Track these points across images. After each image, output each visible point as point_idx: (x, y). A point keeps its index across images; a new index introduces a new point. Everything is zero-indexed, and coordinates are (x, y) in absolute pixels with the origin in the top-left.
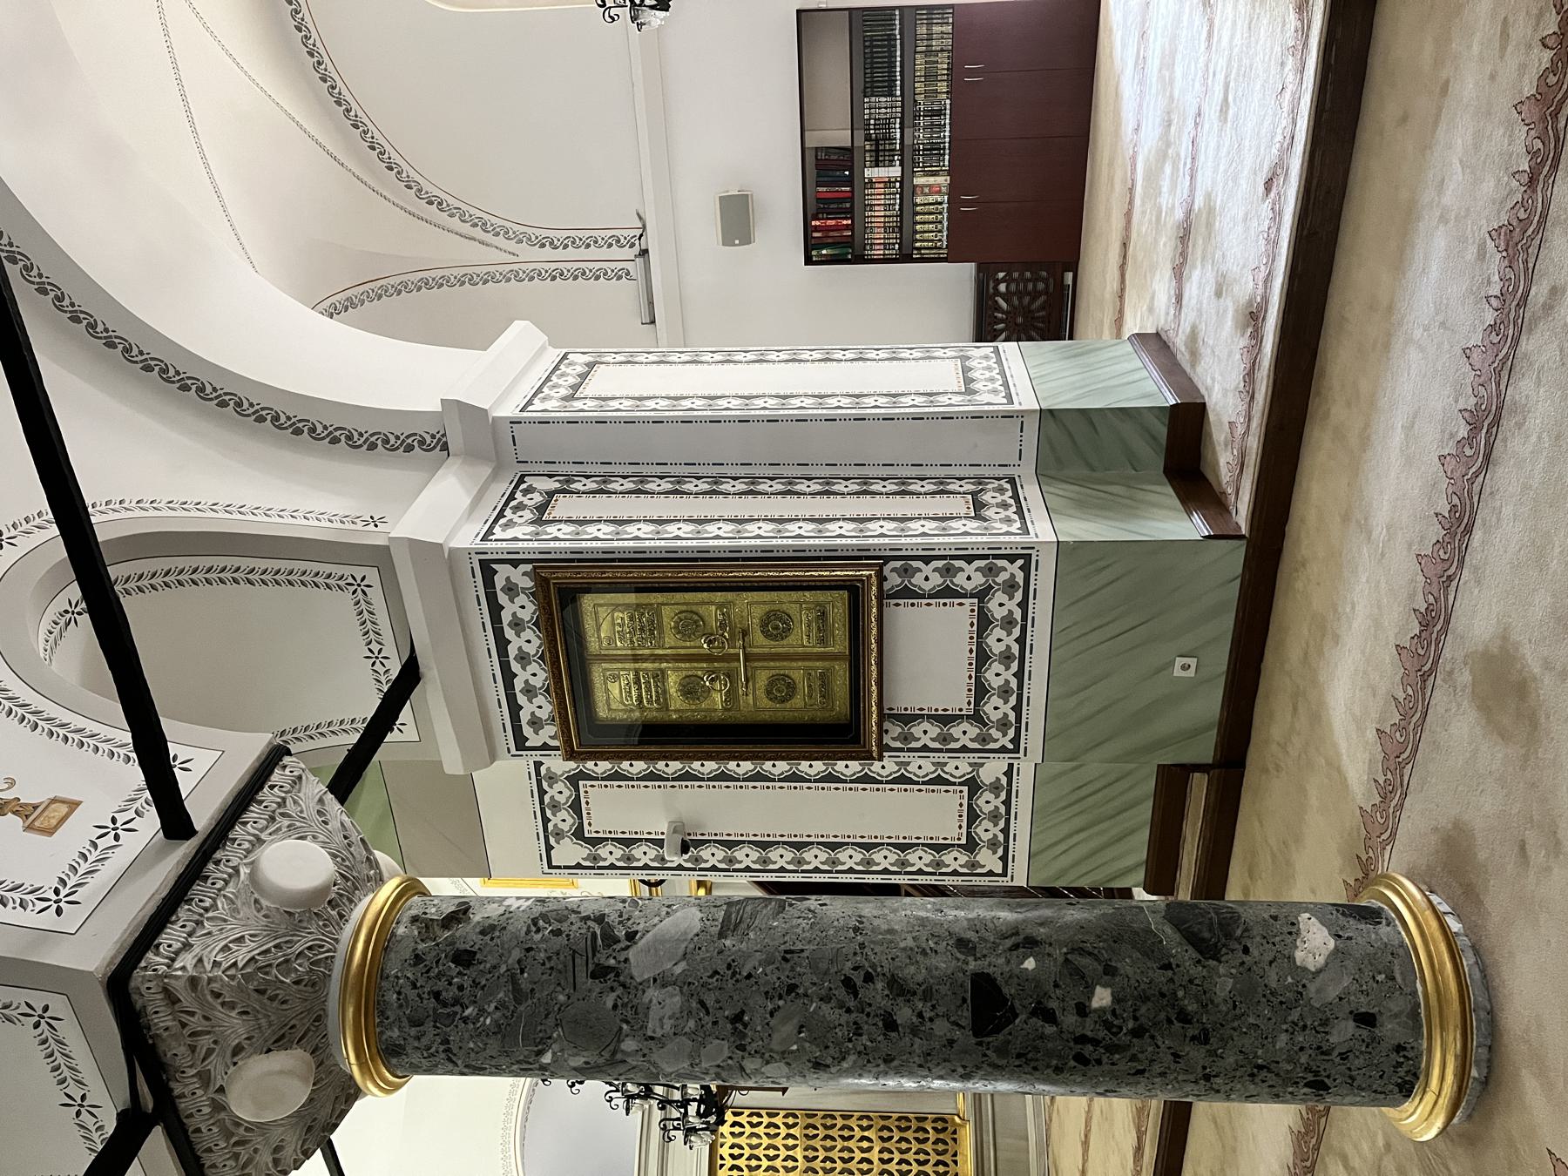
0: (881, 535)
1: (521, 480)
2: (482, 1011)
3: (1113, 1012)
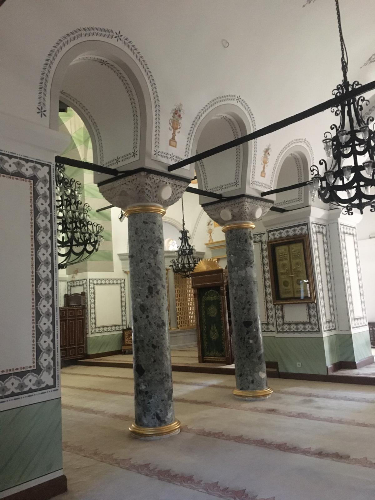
0: (321, 302)
1: (325, 226)
2: (239, 245)
3: (249, 343)
